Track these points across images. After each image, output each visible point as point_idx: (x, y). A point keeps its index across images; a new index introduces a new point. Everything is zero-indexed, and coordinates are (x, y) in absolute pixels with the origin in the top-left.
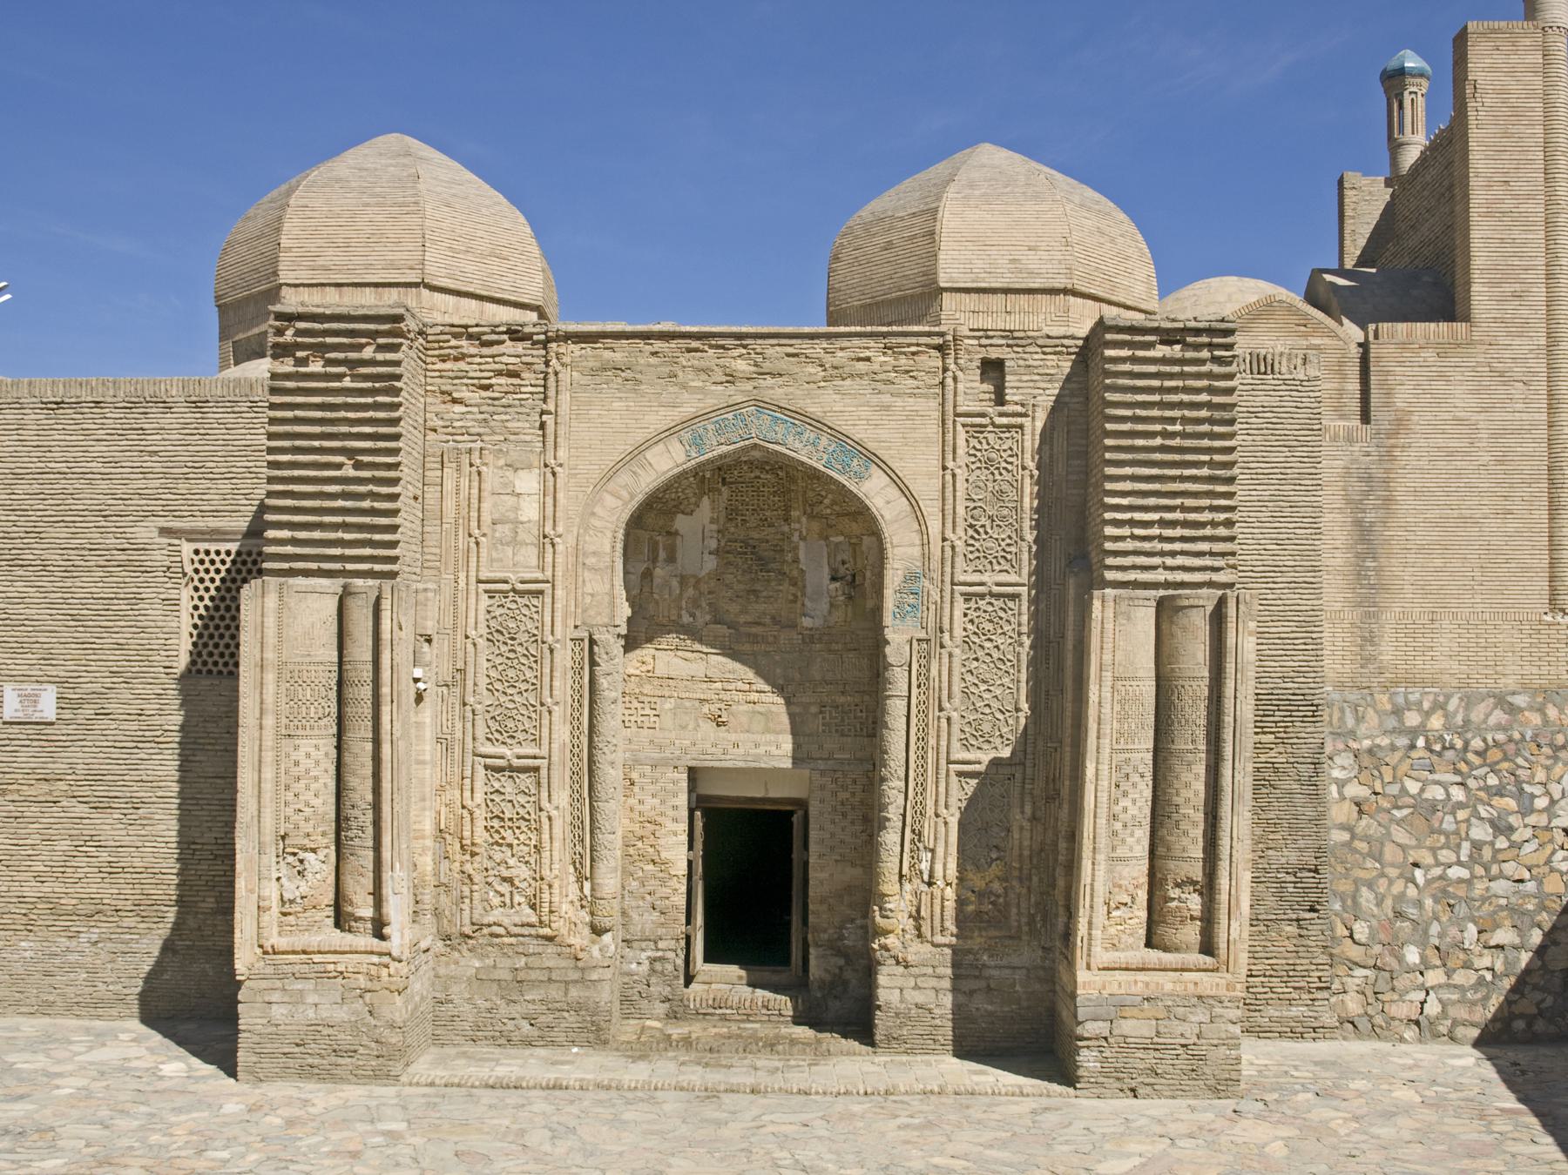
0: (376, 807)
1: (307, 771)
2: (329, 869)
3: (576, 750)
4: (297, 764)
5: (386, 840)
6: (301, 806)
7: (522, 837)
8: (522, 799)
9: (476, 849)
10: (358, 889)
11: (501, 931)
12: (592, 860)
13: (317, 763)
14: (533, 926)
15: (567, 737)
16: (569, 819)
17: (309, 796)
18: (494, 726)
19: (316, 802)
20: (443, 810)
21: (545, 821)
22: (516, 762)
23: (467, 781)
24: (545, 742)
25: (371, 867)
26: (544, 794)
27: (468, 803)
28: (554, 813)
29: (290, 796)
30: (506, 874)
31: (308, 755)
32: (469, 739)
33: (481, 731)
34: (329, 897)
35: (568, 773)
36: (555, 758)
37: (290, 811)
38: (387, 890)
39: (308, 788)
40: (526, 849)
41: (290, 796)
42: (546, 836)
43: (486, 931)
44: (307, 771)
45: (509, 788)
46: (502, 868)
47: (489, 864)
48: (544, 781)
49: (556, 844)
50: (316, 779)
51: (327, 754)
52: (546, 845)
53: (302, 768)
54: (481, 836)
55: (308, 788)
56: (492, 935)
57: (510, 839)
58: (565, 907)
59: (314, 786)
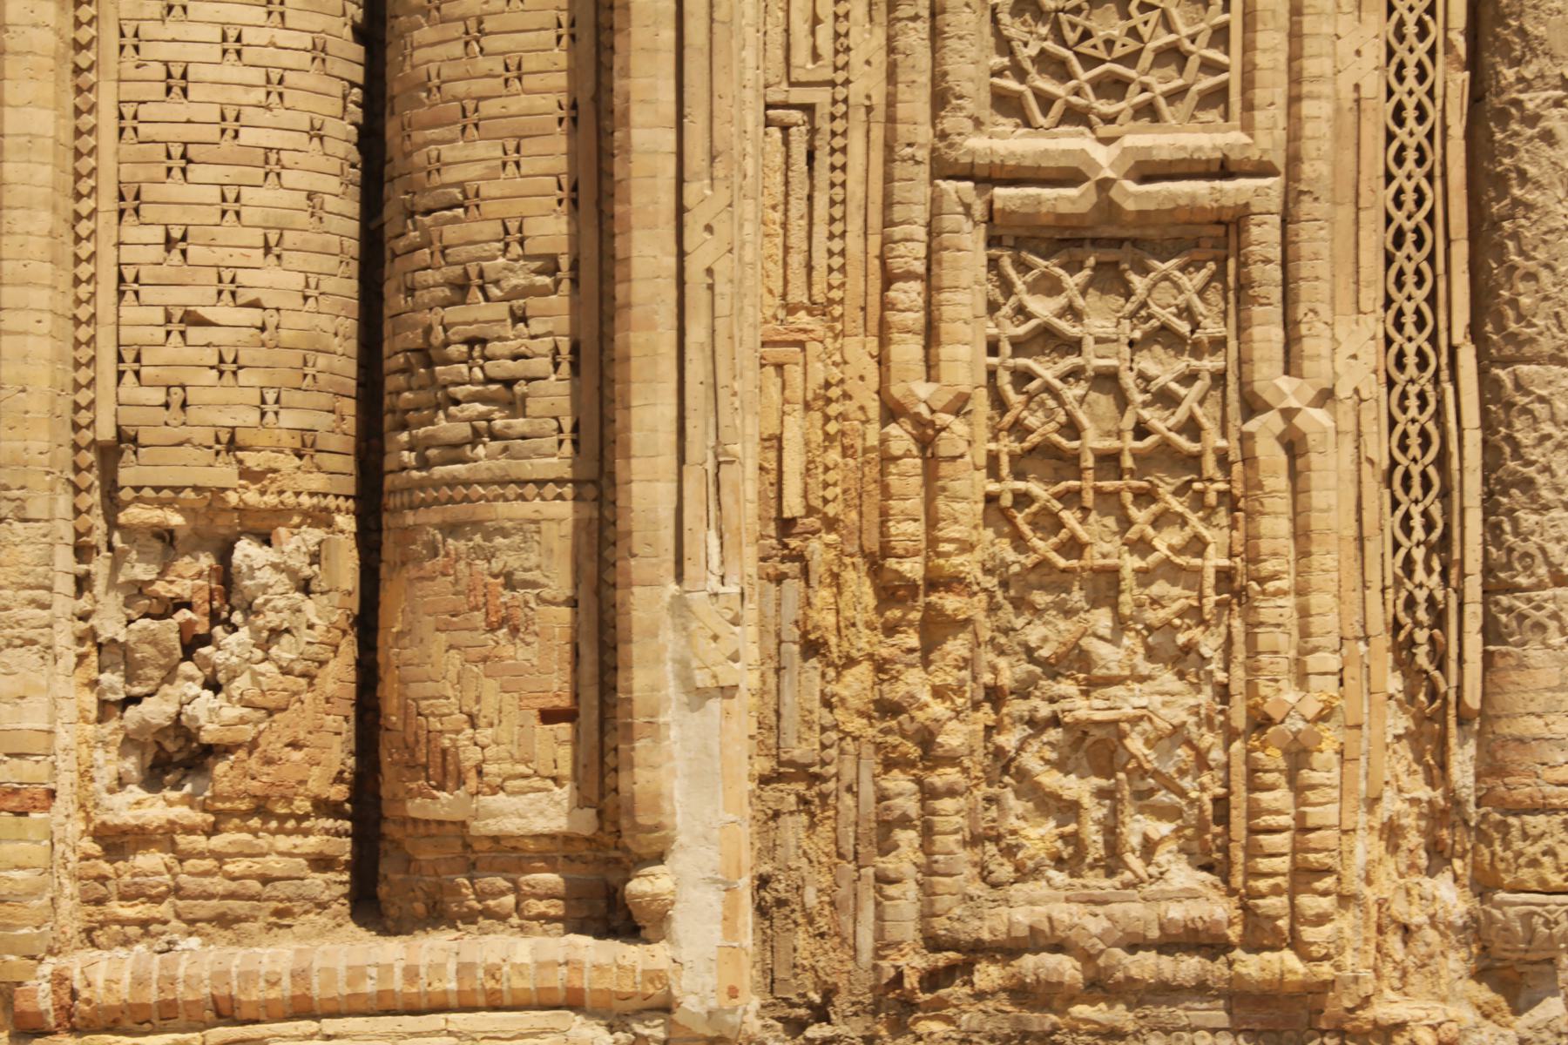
0: (595, 272)
1: (230, 123)
2: (324, 615)
3: (1412, 134)
4: (177, 82)
5: (649, 417)
6: (198, 297)
7: (1165, 541)
8: (1163, 367)
9: (951, 603)
10: (491, 698)
11: (1066, 968)
12: (1491, 631)
13: (276, 85)
14: (1206, 942)
15: (1371, 76)
16: (1378, 447)
17: (235, 245)
18: (1031, 40)
19: (267, 279)
20: (794, 430)
21: (1270, 453)
22: (1133, 195)
23: (909, 294)
24: (1272, 89)
25: (560, 582)
26: (1267, 334)
27: (919, 392)
28: (1315, 420)
29: (143, 240)
30: (1083, 708)
31: (233, 44)
32: (914, 104)
33: (972, 64)
34: (323, 765)
35: (1374, 239)
36: (1314, 169)
37: (141, 320)
38: (650, 677)
39: (230, 205)
40: (1177, 596)
41: (143, 240)
42: (1275, 527)
43: (988, 975)
44: (230, 123)
45: (1101, 319)
46: (1066, 687)
47: (1009, 672)
48: (1268, 276)
49: (1330, 560)
50: (271, 163)
51: (319, 51)
52: (1278, 558)
53: (202, 105)
54: (974, 548)
55: (230, 205)
56: (1021, 993)
57: (1103, 543)
58: (1365, 847)
59: (262, 200)
